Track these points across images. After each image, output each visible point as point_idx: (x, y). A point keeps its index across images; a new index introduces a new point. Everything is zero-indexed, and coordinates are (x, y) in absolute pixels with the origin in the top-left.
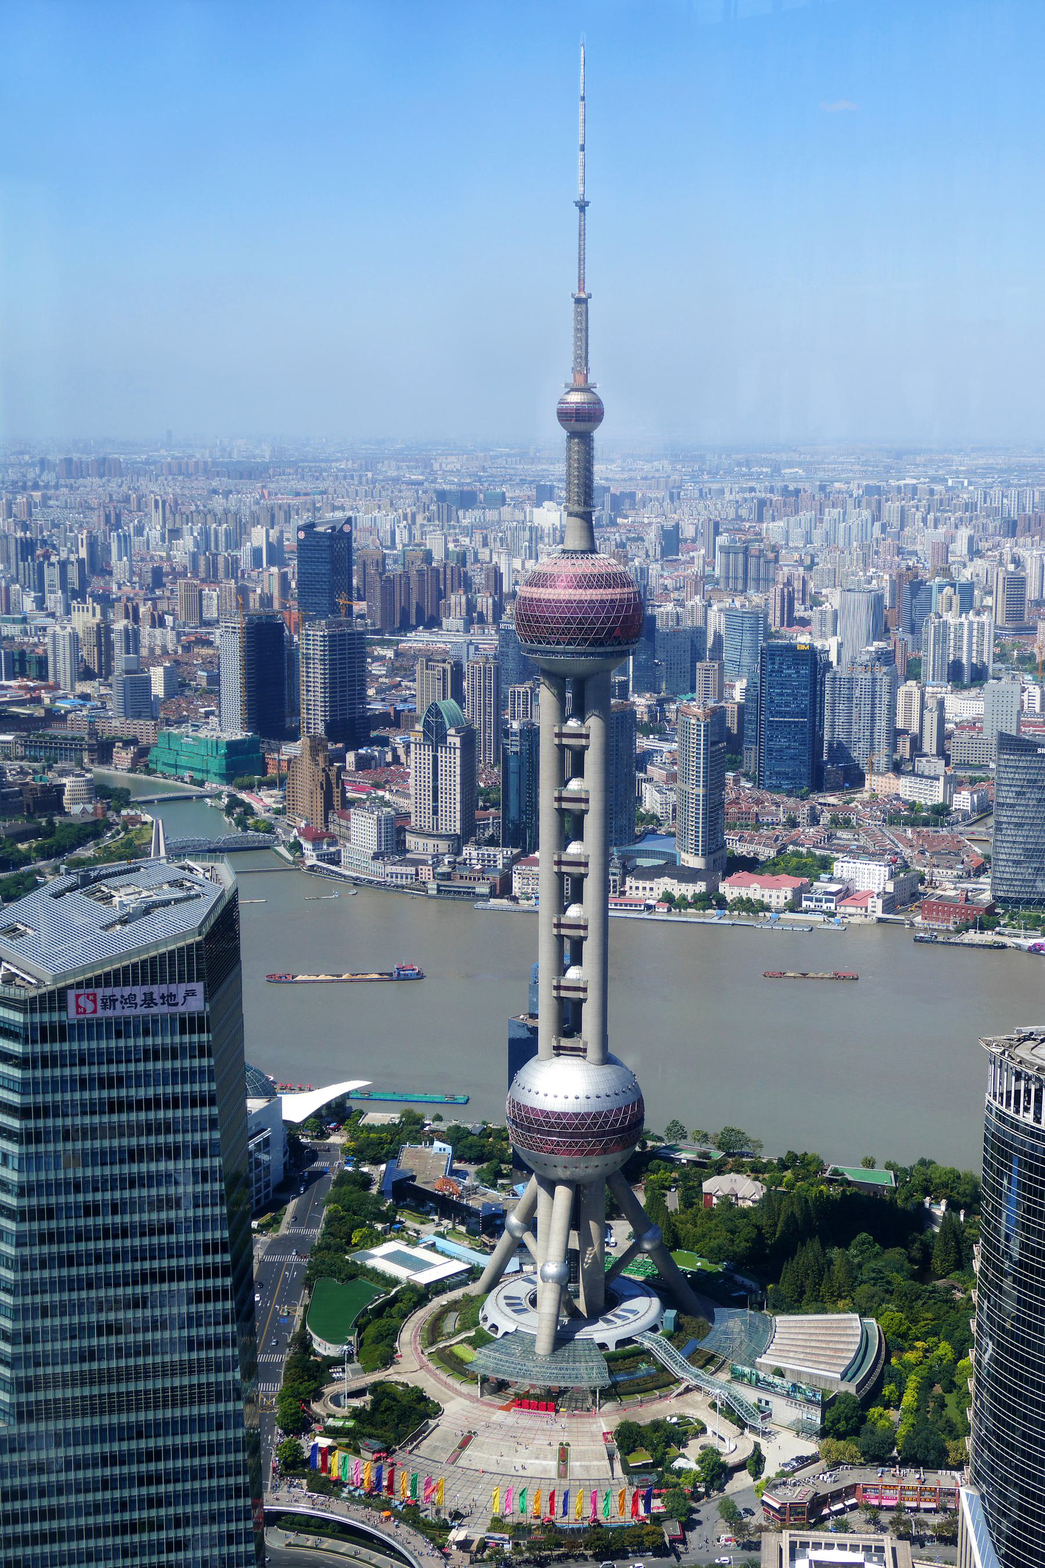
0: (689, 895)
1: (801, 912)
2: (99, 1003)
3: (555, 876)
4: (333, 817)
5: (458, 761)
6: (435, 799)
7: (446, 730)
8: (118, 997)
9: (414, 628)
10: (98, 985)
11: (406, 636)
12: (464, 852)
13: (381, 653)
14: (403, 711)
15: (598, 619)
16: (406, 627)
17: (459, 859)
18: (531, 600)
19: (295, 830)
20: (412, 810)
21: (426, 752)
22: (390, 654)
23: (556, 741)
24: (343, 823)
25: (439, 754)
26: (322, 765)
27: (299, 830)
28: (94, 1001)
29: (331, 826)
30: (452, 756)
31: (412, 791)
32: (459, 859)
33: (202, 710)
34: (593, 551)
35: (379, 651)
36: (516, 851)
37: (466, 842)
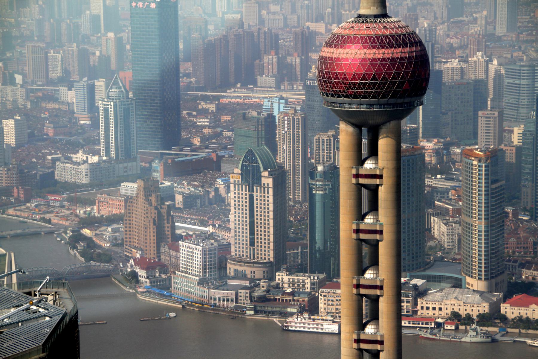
3: (355, 297)
4: (164, 249)
5: (271, 199)
6: (252, 232)
7: (260, 173)
9: (234, 86)
11: (226, 92)
12: (277, 277)
13: (205, 106)
14: (224, 156)
16: (225, 85)
17: (273, 284)
19: (132, 261)
20: (232, 241)
21: (244, 192)
22: (212, 107)
23: (354, 181)
24: (173, 253)
25: (255, 194)
26: (154, 203)
27: (135, 260)
29: (163, 257)
30: (266, 195)
31: (232, 225)
32: (272, 284)
33: (49, 157)
35: (203, 105)
36: (322, 276)
37: (278, 270)
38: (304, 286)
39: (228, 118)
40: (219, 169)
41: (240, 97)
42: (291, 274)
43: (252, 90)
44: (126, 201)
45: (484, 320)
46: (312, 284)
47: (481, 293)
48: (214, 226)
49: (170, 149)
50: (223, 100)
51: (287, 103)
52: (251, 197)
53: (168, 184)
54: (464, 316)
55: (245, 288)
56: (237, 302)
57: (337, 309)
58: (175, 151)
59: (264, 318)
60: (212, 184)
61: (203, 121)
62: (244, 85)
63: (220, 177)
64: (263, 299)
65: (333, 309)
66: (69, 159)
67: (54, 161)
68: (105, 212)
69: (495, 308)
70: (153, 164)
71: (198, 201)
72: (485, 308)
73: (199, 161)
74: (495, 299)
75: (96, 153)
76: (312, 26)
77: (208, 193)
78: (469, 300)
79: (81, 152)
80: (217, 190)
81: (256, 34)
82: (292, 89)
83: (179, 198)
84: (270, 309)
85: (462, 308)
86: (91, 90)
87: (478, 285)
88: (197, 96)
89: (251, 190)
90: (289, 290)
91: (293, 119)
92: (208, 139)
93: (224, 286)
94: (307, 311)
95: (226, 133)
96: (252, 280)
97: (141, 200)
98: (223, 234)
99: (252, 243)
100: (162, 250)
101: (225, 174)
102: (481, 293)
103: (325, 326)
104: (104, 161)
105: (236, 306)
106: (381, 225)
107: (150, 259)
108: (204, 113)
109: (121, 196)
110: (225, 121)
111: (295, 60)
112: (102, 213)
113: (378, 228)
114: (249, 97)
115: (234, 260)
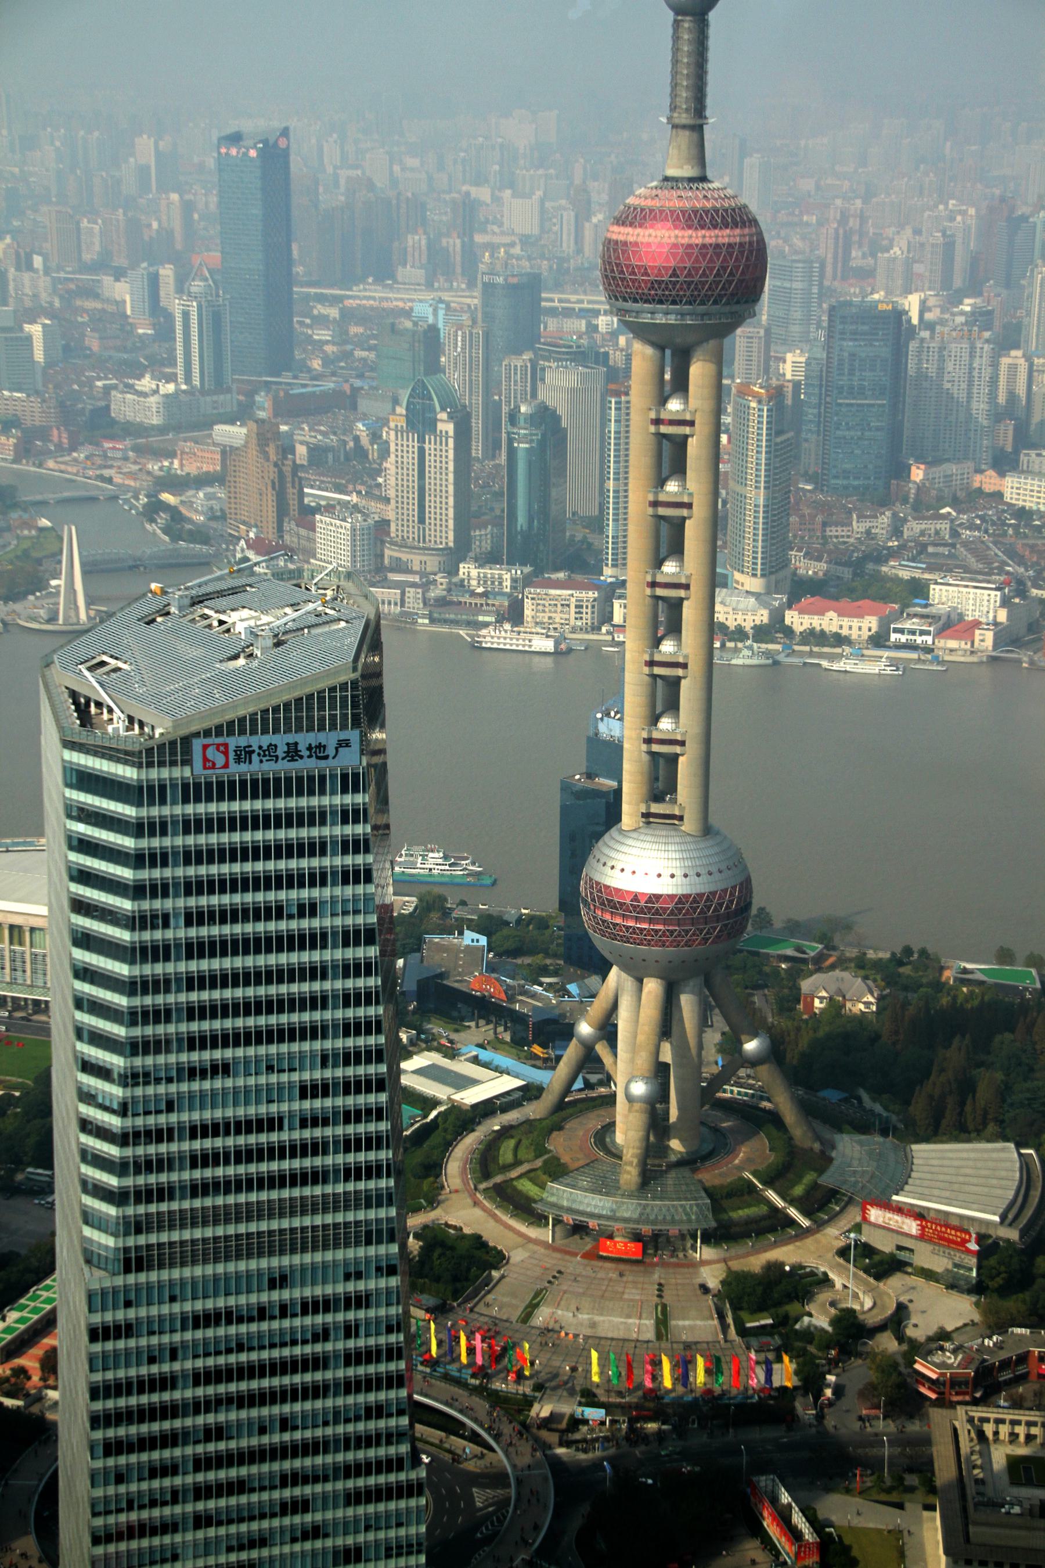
0: (748, 626)
1: (889, 647)
2: (232, 755)
3: (648, 601)
4: (289, 525)
5: (451, 454)
7: (436, 414)
8: (255, 748)
9: (362, 280)
10: (231, 733)
11: (351, 289)
12: (461, 571)
13: (323, 311)
14: (362, 388)
15: (697, 269)
16: (349, 279)
18: (625, 243)
21: (410, 443)
23: (652, 429)
24: (303, 532)
25: (427, 446)
26: (273, 457)
28: (226, 753)
29: (287, 537)
30: (444, 448)
31: (392, 493)
32: (455, 580)
33: (99, 384)
34: (703, 179)
35: (320, 309)
36: (528, 569)
37: (463, 559)
38: (500, 583)
39: (360, 330)
40: (354, 407)
41: (374, 298)
42: (481, 566)
43: (391, 287)
44: (224, 453)
45: (762, 633)
46: (514, 580)
47: (757, 596)
48: (359, 493)
49: (279, 375)
50: (349, 303)
51: (448, 308)
52: (422, 451)
53: (284, 428)
54: (732, 628)
55: (414, 585)
56: (403, 605)
57: (550, 618)
58: (286, 378)
59: (445, 629)
60: (349, 429)
61: (322, 335)
62: (379, 280)
63: (359, 420)
64: (442, 602)
65: (544, 617)
66: (130, 388)
67: (107, 389)
68: (192, 468)
69: (777, 617)
70: (258, 398)
71: (330, 456)
72: (763, 616)
73: (324, 394)
74: (776, 604)
75: (171, 378)
76: (474, 192)
77: (345, 443)
78: (741, 606)
79: (148, 377)
80: (357, 439)
81: (394, 202)
82: (451, 289)
83: (301, 450)
84: (452, 616)
85: (731, 617)
86: (154, 281)
87: (754, 584)
88: (308, 294)
89: (421, 440)
90: (480, 590)
91: (471, 334)
92: (333, 362)
93: (385, 583)
94: (508, 620)
95: (359, 354)
96: (423, 574)
97: (253, 451)
98: (374, 506)
99: (422, 520)
100: (286, 526)
101: (365, 415)
102: (757, 596)
103: (533, 643)
104: (184, 392)
105: (403, 614)
106: (691, 495)
107: (270, 542)
108: (322, 321)
109: (215, 444)
110: (356, 335)
111: (454, 243)
112: (187, 469)
113: (686, 500)
114: (387, 299)
115: (395, 544)
